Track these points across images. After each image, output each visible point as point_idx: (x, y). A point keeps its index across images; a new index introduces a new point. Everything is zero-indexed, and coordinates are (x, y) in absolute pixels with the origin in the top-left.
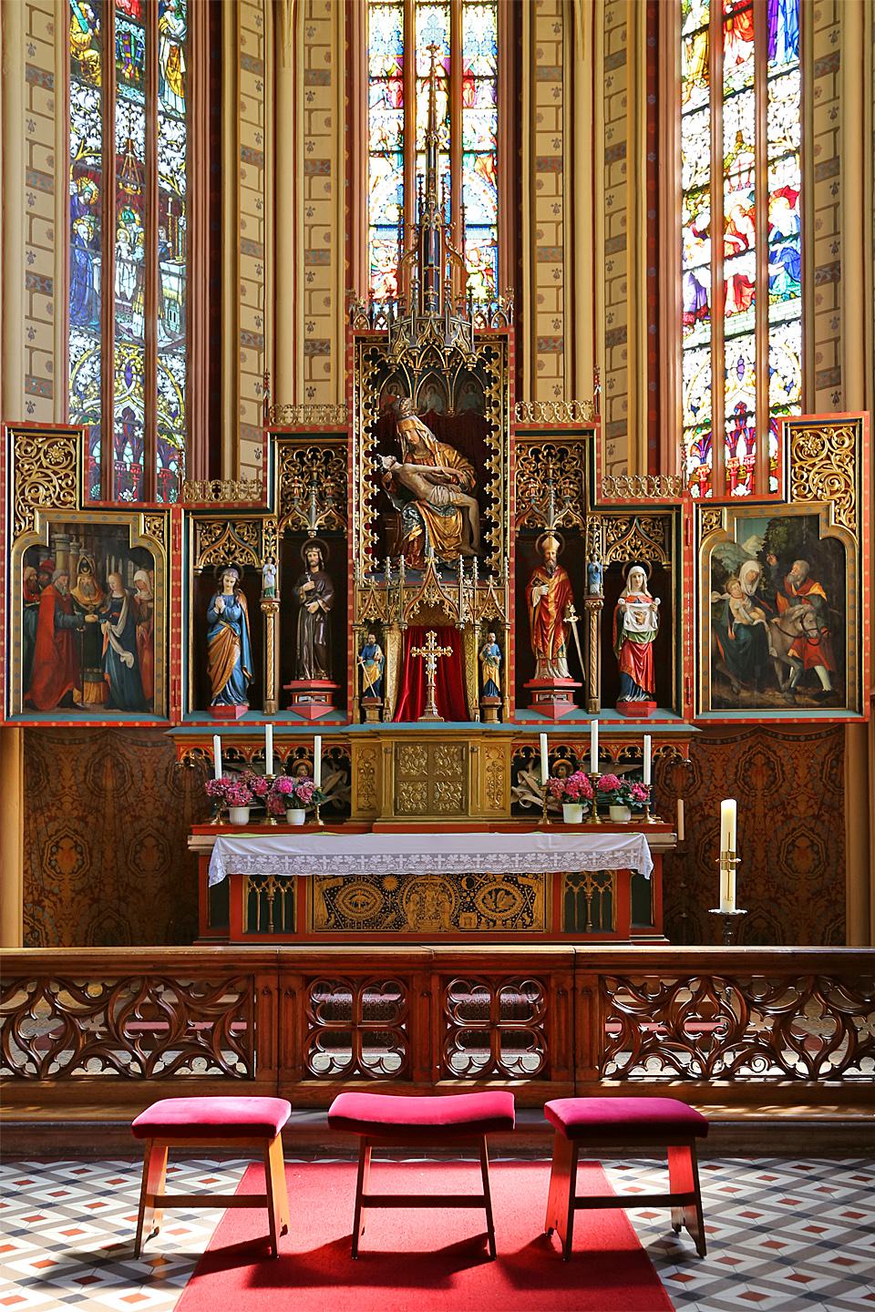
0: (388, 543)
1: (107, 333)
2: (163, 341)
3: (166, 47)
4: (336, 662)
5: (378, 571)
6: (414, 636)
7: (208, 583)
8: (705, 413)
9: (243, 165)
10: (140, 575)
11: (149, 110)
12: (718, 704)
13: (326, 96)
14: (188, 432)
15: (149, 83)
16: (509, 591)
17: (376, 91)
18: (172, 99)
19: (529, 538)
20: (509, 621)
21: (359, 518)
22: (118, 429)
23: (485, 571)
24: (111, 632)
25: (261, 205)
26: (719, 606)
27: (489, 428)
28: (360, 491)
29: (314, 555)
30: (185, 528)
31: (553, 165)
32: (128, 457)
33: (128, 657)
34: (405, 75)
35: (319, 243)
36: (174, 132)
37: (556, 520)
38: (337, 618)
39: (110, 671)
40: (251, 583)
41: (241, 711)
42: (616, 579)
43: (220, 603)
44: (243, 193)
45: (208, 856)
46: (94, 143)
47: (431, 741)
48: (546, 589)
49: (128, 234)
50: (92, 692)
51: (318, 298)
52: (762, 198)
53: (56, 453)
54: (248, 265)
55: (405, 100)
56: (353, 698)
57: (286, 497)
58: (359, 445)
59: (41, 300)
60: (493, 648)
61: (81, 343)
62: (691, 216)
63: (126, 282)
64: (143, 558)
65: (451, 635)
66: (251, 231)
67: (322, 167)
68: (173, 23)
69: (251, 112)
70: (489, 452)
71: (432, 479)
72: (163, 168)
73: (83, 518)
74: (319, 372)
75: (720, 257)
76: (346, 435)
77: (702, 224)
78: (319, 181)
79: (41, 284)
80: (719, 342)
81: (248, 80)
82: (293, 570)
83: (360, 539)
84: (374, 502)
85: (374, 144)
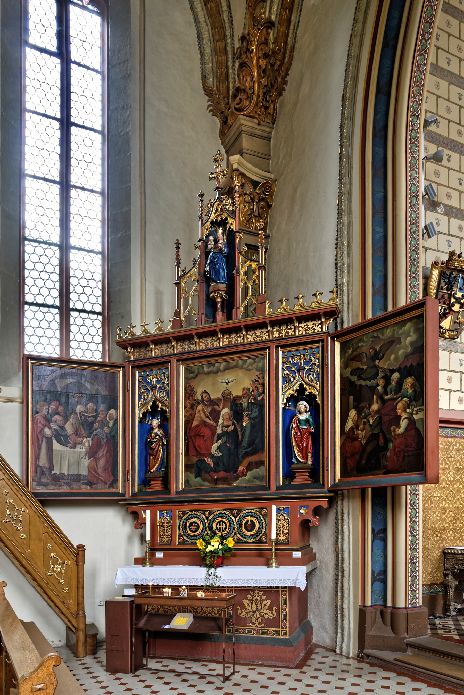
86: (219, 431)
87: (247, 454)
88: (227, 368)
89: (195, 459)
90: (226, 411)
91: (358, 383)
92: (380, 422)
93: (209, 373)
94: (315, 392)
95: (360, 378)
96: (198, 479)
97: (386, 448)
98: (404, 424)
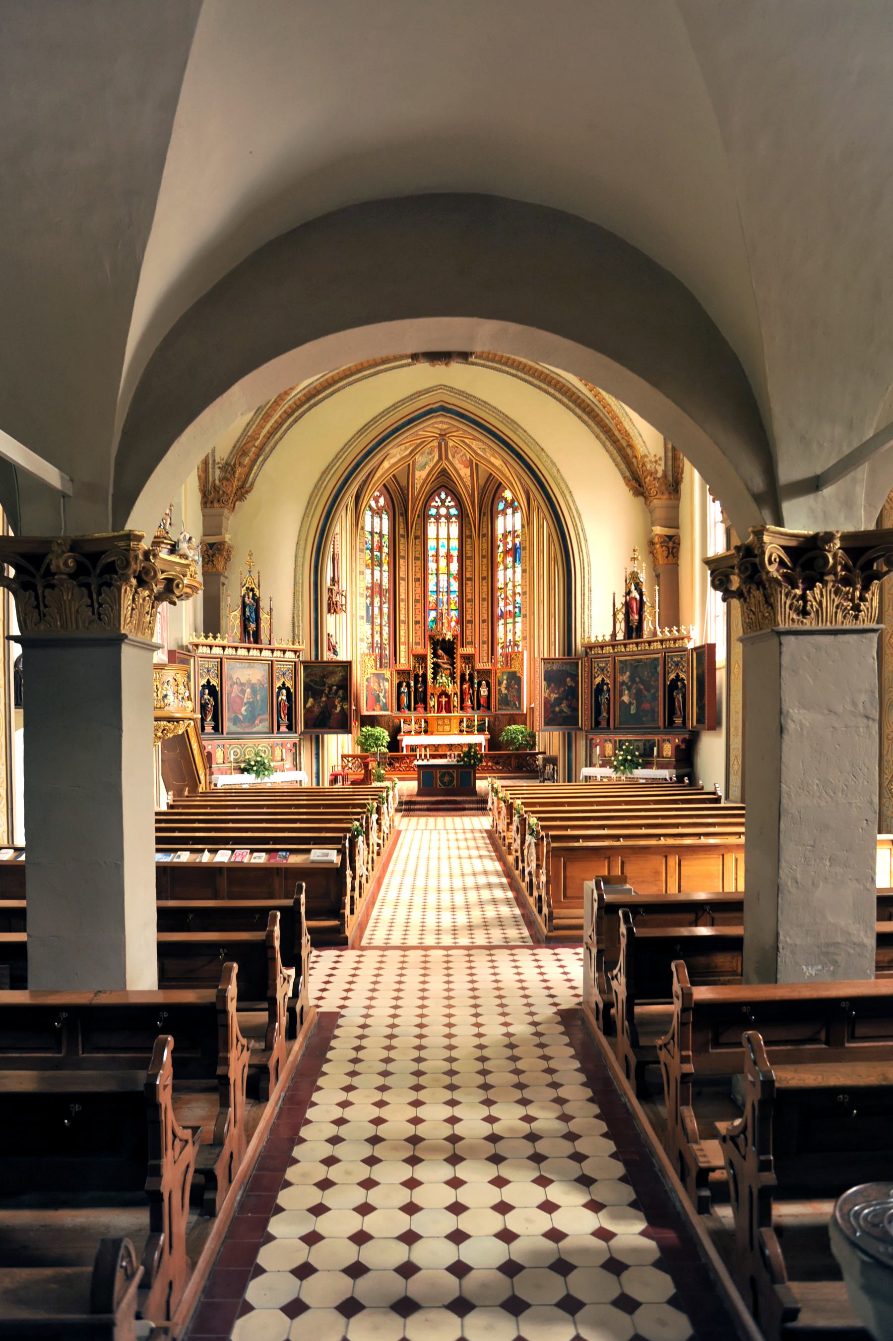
0: (435, 674)
1: (373, 623)
2: (384, 623)
3: (384, 555)
4: (425, 702)
5: (433, 682)
6: (440, 697)
7: (399, 685)
8: (503, 640)
9: (401, 581)
10: (386, 684)
11: (381, 571)
12: (499, 709)
13: (419, 563)
14: (389, 644)
15: (381, 565)
16: (459, 686)
17: (430, 559)
18: (385, 567)
19: (463, 676)
20: (459, 694)
21: (430, 672)
22: (375, 645)
23: (454, 682)
24: (381, 695)
25: (405, 590)
26: (500, 690)
27: (455, 653)
28: (430, 665)
29: (420, 679)
30: (395, 674)
31: (470, 579)
32: (377, 651)
33: (384, 700)
34: (437, 555)
35: (417, 598)
36: (385, 574)
37: (468, 672)
38: (425, 691)
39: (381, 703)
40: (408, 685)
41: (407, 711)
42: (480, 684)
43: (402, 689)
44: (401, 588)
45: (402, 741)
46: (370, 581)
47: (444, 718)
48: (465, 686)
49: (377, 600)
50: (378, 707)
51: (417, 611)
52: (514, 594)
53: (371, 659)
54: (402, 604)
55: (437, 561)
56: (428, 708)
57: (415, 667)
58: (430, 656)
59: (362, 621)
60: (455, 698)
61: (368, 627)
62: (500, 595)
63: (376, 611)
64: (387, 680)
65: (447, 696)
66: (402, 596)
67: (417, 580)
68: (385, 550)
69: (403, 568)
70: (455, 658)
71: (443, 663)
72: (384, 584)
73: (376, 672)
74: (418, 628)
75: (506, 605)
76: (427, 655)
77: (503, 596)
78: (417, 583)
79: (362, 618)
80: (506, 624)
81: (402, 561)
82: (416, 683)
83: (430, 675)
84: (432, 668)
85: (430, 572)
86: (245, 701)
87: (259, 715)
88: (248, 667)
89: (233, 715)
90: (248, 690)
91: (315, 686)
92: (326, 706)
93: (240, 668)
94: (290, 687)
95: (315, 684)
96: (235, 727)
97: (330, 718)
98: (339, 709)
